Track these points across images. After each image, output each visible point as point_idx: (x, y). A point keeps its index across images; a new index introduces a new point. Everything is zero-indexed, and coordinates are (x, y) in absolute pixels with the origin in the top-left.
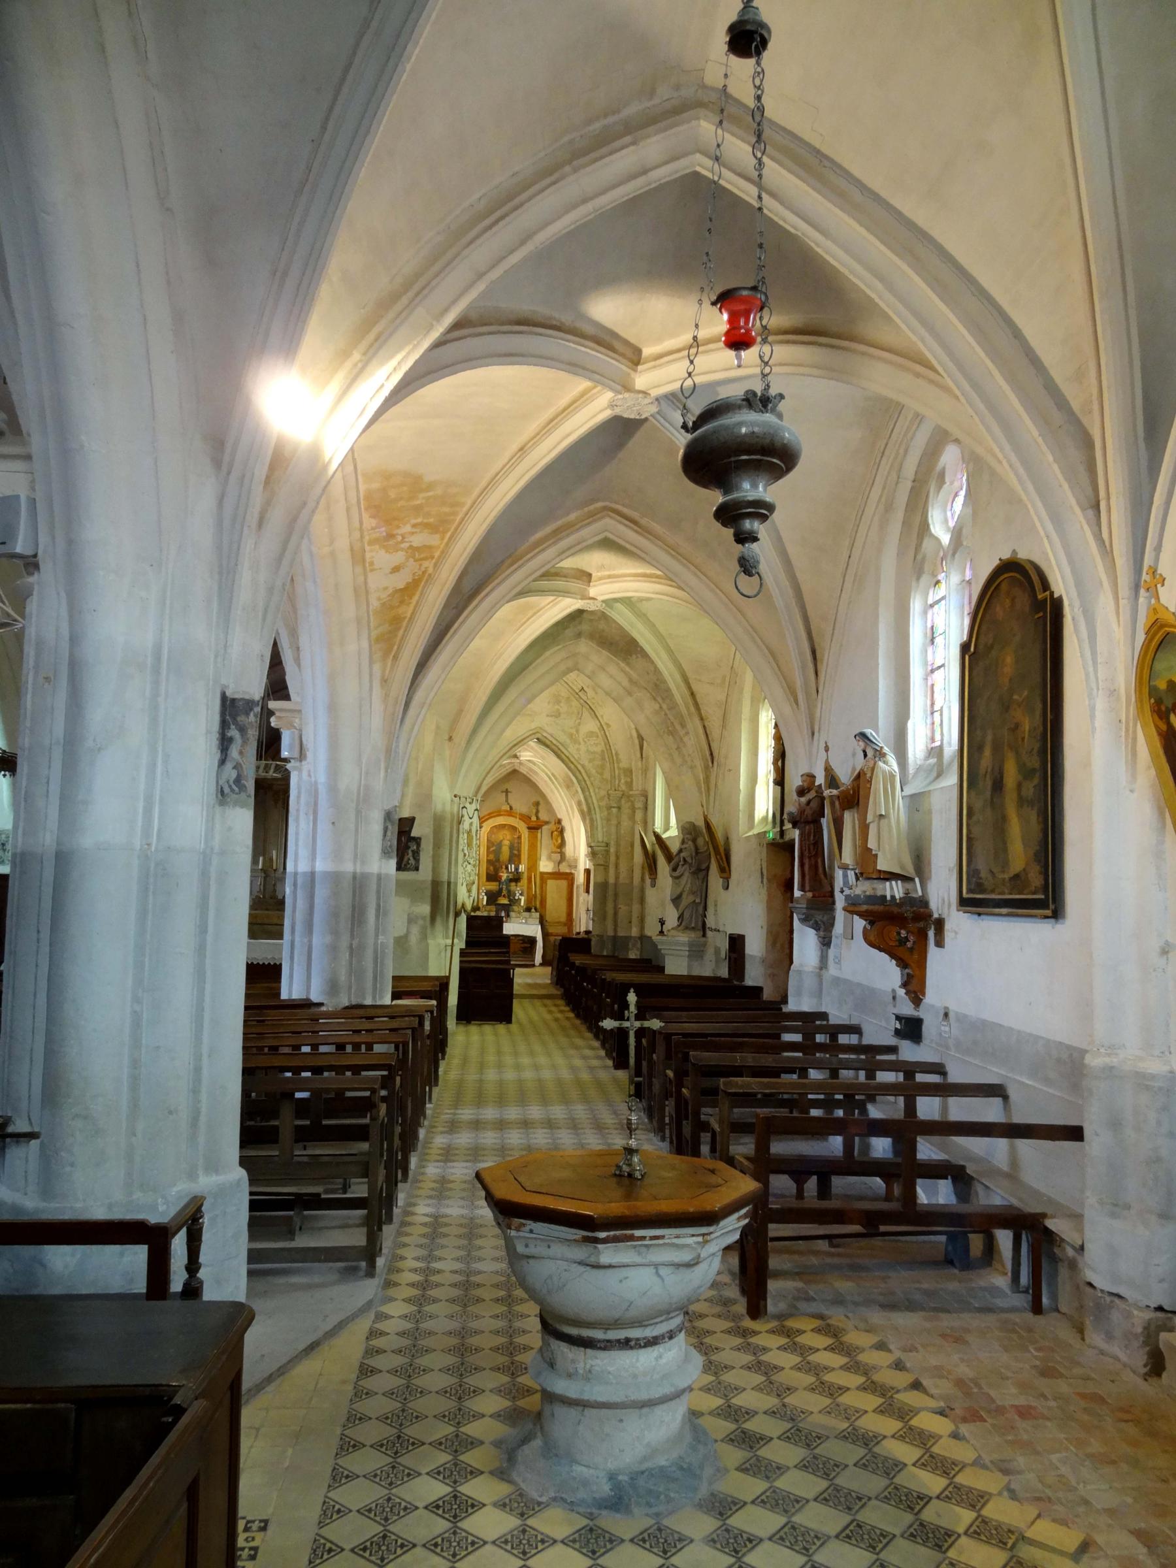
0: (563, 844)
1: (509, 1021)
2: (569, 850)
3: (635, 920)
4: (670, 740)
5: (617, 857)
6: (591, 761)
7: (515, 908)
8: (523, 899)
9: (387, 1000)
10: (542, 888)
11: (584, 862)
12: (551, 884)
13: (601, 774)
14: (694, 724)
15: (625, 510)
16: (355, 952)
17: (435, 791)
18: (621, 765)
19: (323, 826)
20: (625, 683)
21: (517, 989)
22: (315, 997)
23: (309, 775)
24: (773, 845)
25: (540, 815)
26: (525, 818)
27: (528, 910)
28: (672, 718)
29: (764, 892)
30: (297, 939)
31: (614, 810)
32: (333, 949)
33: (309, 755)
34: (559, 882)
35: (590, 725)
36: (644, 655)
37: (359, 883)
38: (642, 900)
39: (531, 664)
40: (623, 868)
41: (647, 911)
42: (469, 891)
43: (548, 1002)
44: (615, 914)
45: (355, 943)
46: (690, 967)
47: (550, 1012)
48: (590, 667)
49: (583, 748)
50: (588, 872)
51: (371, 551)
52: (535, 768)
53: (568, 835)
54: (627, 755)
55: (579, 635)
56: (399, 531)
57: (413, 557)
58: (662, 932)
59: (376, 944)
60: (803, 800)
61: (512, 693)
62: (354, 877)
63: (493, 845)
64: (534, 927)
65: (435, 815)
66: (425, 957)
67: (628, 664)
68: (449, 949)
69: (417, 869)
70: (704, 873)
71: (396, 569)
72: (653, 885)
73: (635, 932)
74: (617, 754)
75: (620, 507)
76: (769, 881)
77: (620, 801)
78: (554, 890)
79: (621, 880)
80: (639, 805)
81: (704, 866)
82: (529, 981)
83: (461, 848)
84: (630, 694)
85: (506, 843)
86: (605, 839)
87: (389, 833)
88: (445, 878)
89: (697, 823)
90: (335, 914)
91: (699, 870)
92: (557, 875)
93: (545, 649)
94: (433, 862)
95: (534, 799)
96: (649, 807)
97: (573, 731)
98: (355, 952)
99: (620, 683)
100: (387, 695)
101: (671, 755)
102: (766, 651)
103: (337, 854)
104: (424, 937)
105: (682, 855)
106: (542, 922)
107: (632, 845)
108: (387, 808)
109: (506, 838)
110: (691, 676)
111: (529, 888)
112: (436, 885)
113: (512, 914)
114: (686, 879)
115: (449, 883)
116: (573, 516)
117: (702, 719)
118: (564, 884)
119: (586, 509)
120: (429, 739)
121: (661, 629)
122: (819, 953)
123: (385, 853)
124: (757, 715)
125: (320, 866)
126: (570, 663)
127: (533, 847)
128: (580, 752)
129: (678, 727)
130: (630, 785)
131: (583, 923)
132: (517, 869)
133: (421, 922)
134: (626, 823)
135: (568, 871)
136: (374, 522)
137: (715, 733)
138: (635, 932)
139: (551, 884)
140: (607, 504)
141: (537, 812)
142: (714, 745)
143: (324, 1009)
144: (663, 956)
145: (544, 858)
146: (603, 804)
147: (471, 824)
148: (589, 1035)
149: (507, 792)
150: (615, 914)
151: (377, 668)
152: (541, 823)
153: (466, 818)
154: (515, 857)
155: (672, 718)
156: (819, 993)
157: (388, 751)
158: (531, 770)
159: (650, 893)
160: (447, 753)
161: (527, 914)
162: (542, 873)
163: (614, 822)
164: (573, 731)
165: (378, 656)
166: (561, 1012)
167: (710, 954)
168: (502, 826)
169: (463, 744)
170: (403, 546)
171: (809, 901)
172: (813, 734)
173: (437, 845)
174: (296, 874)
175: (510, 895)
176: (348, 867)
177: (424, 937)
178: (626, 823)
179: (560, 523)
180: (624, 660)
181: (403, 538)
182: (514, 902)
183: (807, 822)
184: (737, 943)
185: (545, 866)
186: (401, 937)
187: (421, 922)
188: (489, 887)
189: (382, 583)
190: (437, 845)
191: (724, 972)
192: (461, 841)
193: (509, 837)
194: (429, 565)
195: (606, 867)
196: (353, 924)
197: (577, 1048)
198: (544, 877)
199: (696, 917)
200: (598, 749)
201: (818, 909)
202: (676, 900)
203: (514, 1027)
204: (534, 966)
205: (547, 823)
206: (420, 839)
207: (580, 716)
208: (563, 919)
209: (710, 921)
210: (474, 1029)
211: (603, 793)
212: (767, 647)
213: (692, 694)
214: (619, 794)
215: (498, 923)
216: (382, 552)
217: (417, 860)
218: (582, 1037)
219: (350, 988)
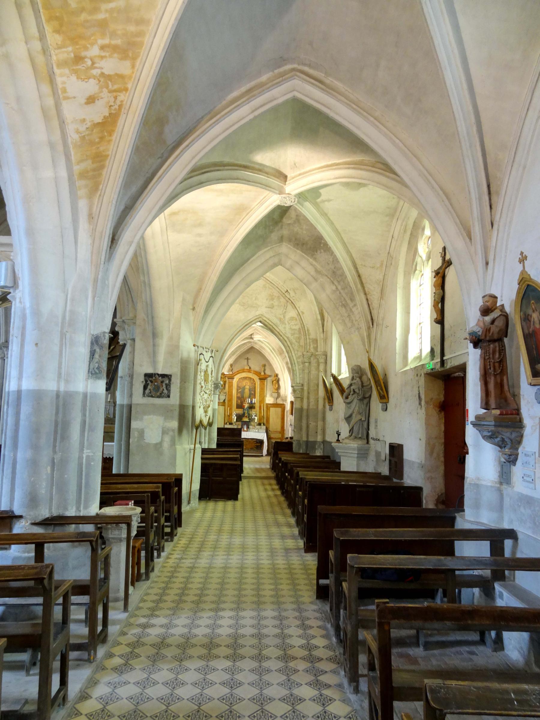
0: (279, 388)
1: (236, 499)
2: (282, 391)
3: (320, 431)
4: (343, 310)
5: (308, 393)
6: (293, 334)
7: (252, 423)
8: (256, 418)
9: (94, 509)
11: (290, 398)
12: (272, 410)
13: (299, 342)
14: (360, 298)
15: (311, 71)
16: (58, 465)
17: (182, 343)
18: (311, 337)
19: (29, 348)
20: (313, 272)
21: (245, 474)
23: (20, 302)
24: (432, 375)
25: (266, 372)
26: (257, 373)
27: (260, 424)
28: (344, 295)
29: (422, 413)
30: (6, 453)
31: (307, 364)
32: (34, 464)
33: (20, 283)
35: (292, 313)
36: (327, 248)
37: (62, 402)
38: (324, 419)
39: (249, 259)
40: (312, 400)
41: (327, 426)
42: (206, 412)
43: (266, 482)
44: (308, 427)
45: (57, 457)
46: (358, 465)
47: (266, 490)
48: (289, 263)
49: (287, 327)
50: (292, 403)
51: (61, 75)
52: (263, 345)
53: (281, 383)
54: (314, 331)
55: (281, 239)
57: (107, 87)
58: (338, 440)
59: (80, 458)
60: (488, 319)
61: (236, 280)
62: (58, 396)
64: (262, 434)
65: (181, 359)
66: (174, 457)
67: (315, 259)
68: (192, 451)
69: (169, 396)
70: (368, 399)
71: (91, 100)
72: (331, 409)
73: (319, 439)
74: (308, 330)
75: (306, 69)
76: (427, 402)
77: (310, 359)
78: (274, 413)
79: (311, 407)
80: (322, 360)
81: (367, 395)
82: (257, 466)
83: (198, 382)
84: (316, 280)
85: (247, 387)
86: (301, 382)
87: (97, 356)
88: (191, 403)
89: (362, 366)
90: (36, 430)
91: (364, 398)
92: (275, 405)
93: (258, 248)
94: (180, 392)
95: (264, 362)
96: (328, 362)
97: (282, 317)
98: (58, 465)
99: (309, 273)
100: (94, 230)
101: (344, 321)
102: (441, 193)
103: (40, 373)
104: (173, 444)
105: (352, 387)
106: (267, 431)
107: (318, 386)
108: (95, 332)
109: (247, 385)
110: (359, 263)
111: (260, 412)
112: (183, 408)
113: (251, 427)
114: (356, 405)
115: (193, 407)
116: (264, 78)
117: (365, 294)
118: (279, 410)
119: (276, 71)
120: (178, 306)
121: (338, 226)
122: (499, 469)
123: (93, 373)
124: (409, 283)
126: (276, 260)
127: (262, 389)
128: (286, 329)
129: (349, 302)
130: (316, 349)
131: (289, 433)
132: (251, 401)
134: (314, 372)
135: (281, 403)
136: (59, 38)
137: (375, 304)
138: (319, 439)
139: (272, 410)
140: (295, 66)
141: (265, 370)
142: (375, 313)
144: (340, 457)
145: (268, 395)
146: (300, 360)
147: (207, 366)
148: (288, 511)
149: (248, 359)
150: (308, 427)
151: (83, 204)
152: (266, 376)
153: (203, 361)
154: (252, 395)
155: (344, 295)
156: (500, 508)
157: (96, 281)
158: (261, 347)
159: (330, 416)
160: (192, 318)
162: (267, 404)
163: (306, 371)
164: (282, 317)
165: (82, 192)
166: (273, 490)
167: (372, 457)
168: (245, 378)
169: (202, 312)
170: (95, 72)
171: (496, 418)
172: (487, 264)
173: (184, 379)
174: (19, 392)
175: (249, 416)
176: (51, 385)
177: (173, 444)
178: (314, 372)
179: (253, 84)
180: (312, 256)
181: (93, 63)
182: (251, 420)
183: (493, 341)
184: (396, 450)
185: (269, 400)
186: (156, 444)
187: (171, 433)
189: (78, 115)
190: (184, 379)
191: (385, 470)
192: (199, 377)
193: (248, 384)
194: (122, 97)
195: (302, 399)
196: (55, 440)
197: (278, 525)
198: (269, 406)
199: (362, 430)
200: (297, 327)
201: (507, 427)
202: (348, 419)
203: (238, 503)
204: (262, 456)
205: (270, 376)
206: (171, 376)
207: (286, 307)
208: (279, 429)
209: (372, 433)
210: (211, 505)
211: (300, 354)
212: (442, 189)
213: (359, 276)
214: (309, 354)
215: (238, 432)
216: (74, 78)
218: (284, 514)
219: (51, 499)
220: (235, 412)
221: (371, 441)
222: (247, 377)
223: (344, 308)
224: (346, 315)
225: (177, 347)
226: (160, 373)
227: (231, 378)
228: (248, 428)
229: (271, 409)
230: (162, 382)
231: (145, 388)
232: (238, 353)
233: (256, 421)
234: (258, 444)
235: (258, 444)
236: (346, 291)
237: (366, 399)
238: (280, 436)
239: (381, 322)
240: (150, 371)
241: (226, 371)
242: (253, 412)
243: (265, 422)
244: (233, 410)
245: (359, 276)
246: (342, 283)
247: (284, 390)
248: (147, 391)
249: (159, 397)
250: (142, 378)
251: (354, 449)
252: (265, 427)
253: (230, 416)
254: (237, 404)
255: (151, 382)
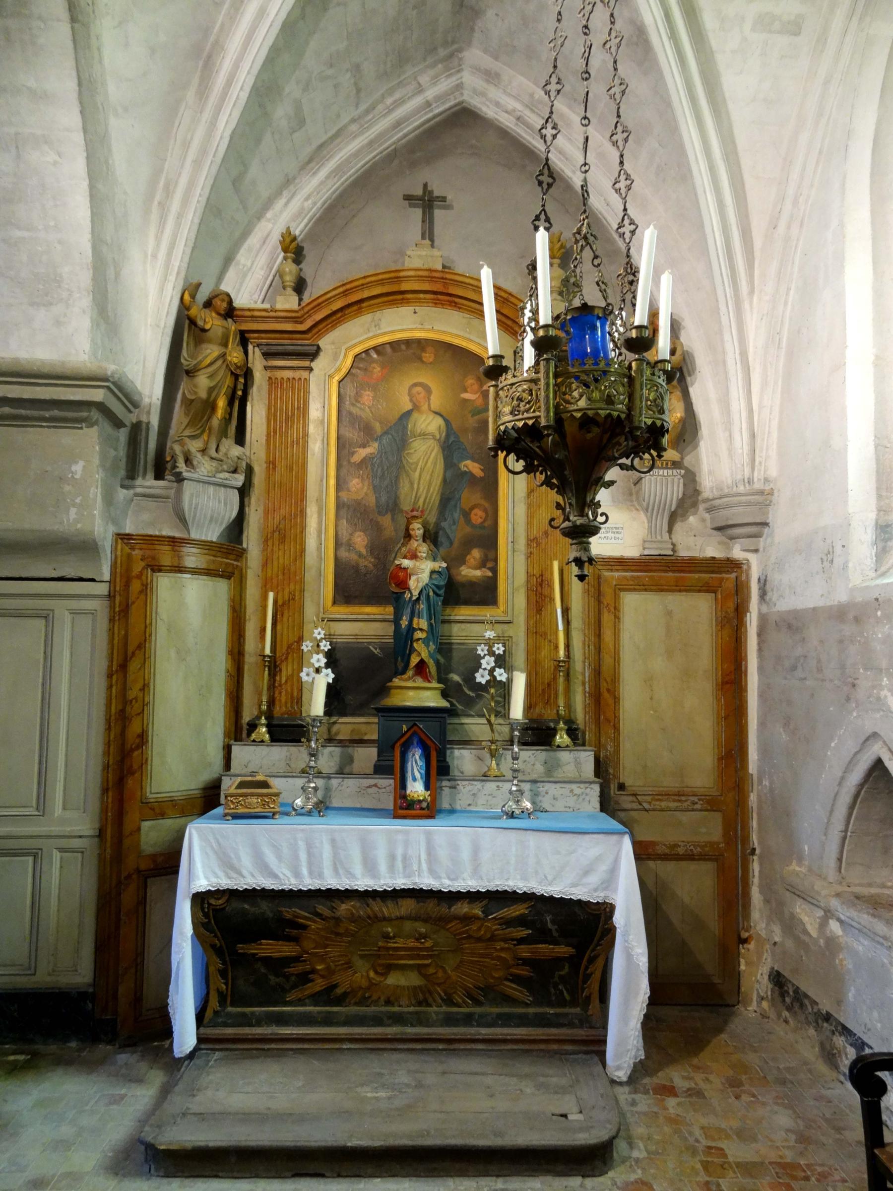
7: (475, 726)
8: (520, 683)
10: (596, 628)
12: (639, 610)
27: (538, 734)
34: (678, 602)
63: (367, 429)
78: (655, 641)
85: (429, 424)
92: (663, 571)
111: (538, 631)
113: (463, 759)
118: (698, 610)
135: (712, 550)
139: (639, 610)
149: (427, 203)
161: (532, 759)
188: (346, 631)
208: (702, 773)
220: (327, 626)
222: (420, 344)
227: (294, 344)
228: (439, 770)
229: (631, 602)
232: (353, 152)
233: (517, 710)
234: (545, 949)
235: (545, 949)
238: (711, 829)
241: (250, 283)
242: (473, 628)
243: (580, 715)
244: (310, 611)
247: (741, 442)
252: (586, 759)
253: (281, 663)
254: (340, 567)
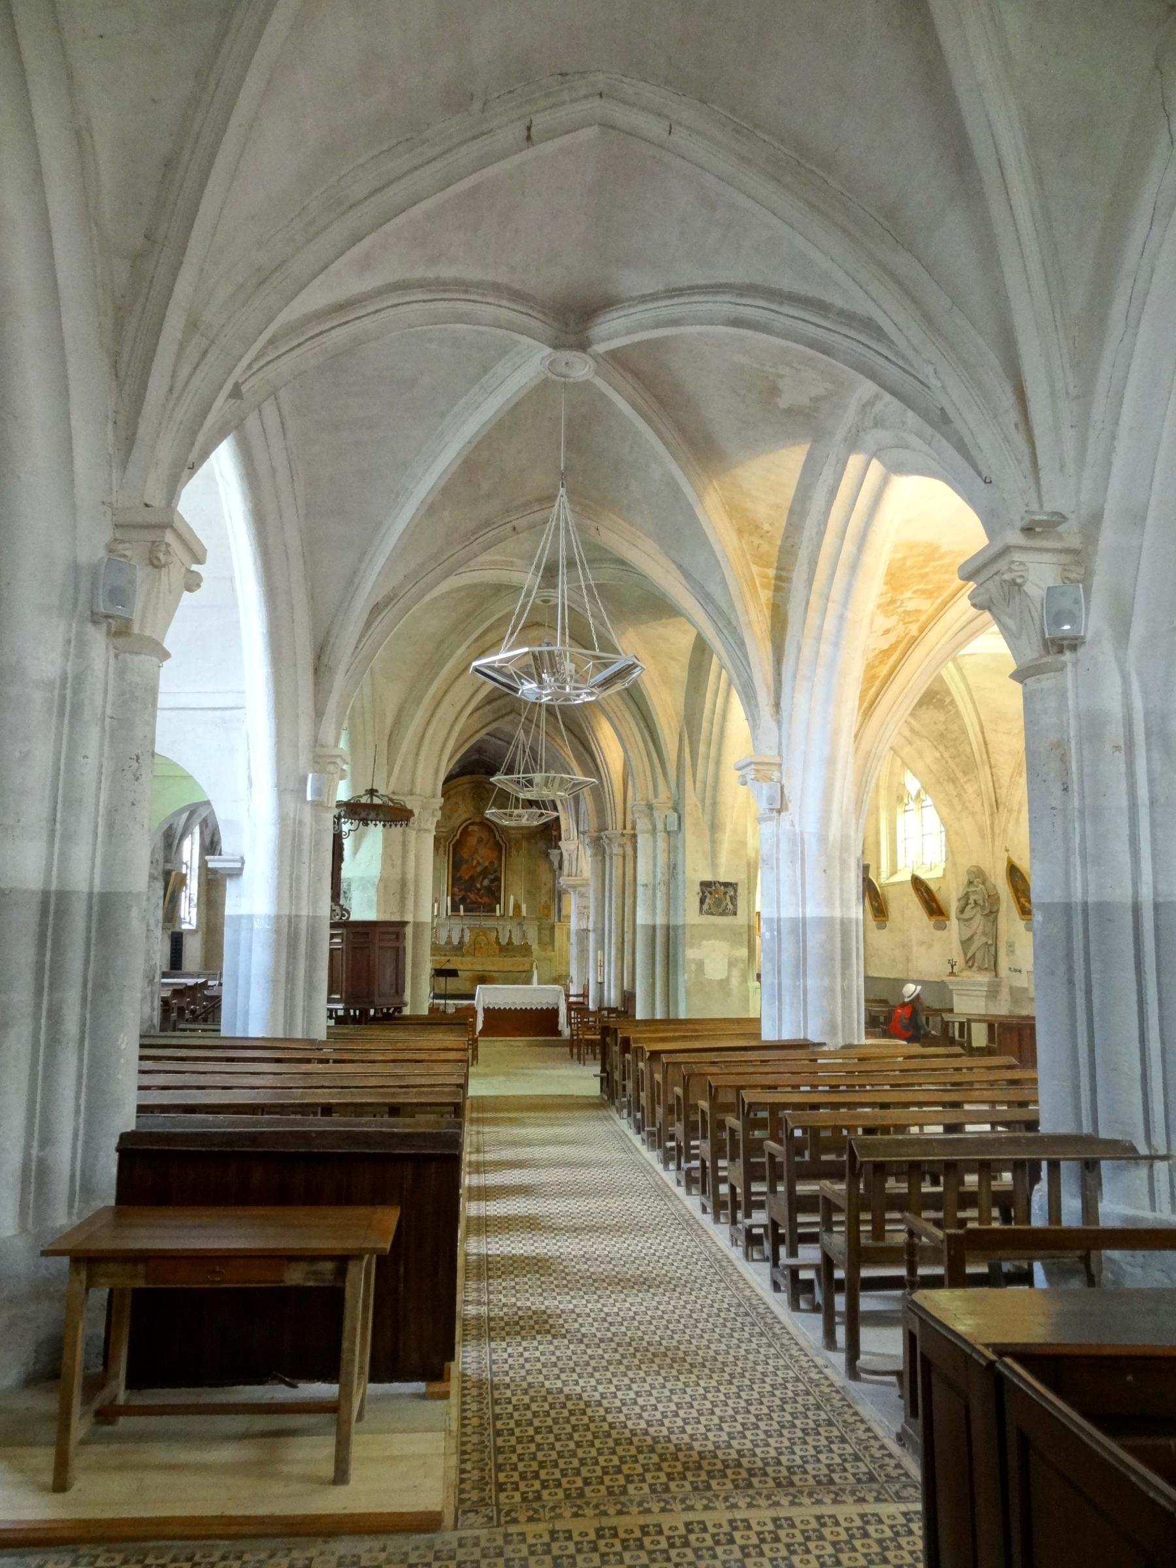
4: (950, 787)
20: (907, 733)
22: (813, 1037)
28: (953, 766)
33: (793, 806)
46: (986, 1006)
56: (901, 597)
58: (952, 974)
66: (746, 999)
69: (735, 914)
71: (887, 632)
84: (910, 743)
91: (991, 912)
103: (829, 901)
105: (972, 898)
114: (978, 922)
125: (812, 911)
129: (960, 775)
133: (741, 965)
142: (1002, 793)
143: (825, 1048)
176: (837, 913)
186: (721, 980)
187: (741, 965)
217: (735, 905)
221: (1003, 970)
223: (951, 785)
224: (955, 793)
225: (743, 844)
226: (722, 880)
230: (725, 893)
231: (702, 902)
236: (958, 760)
237: (992, 914)
239: (1016, 808)
240: (708, 877)
245: (985, 742)
246: (952, 750)
248: (705, 907)
249: (721, 914)
250: (697, 888)
251: (981, 985)
255: (710, 893)
